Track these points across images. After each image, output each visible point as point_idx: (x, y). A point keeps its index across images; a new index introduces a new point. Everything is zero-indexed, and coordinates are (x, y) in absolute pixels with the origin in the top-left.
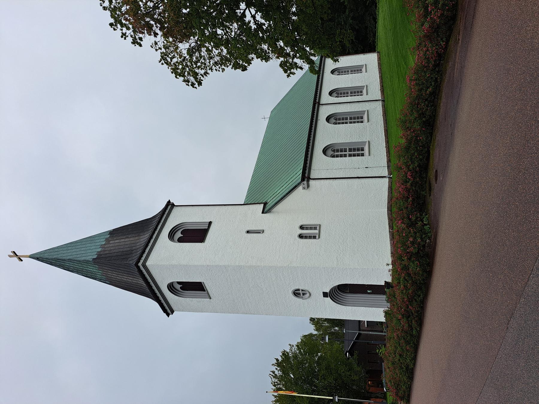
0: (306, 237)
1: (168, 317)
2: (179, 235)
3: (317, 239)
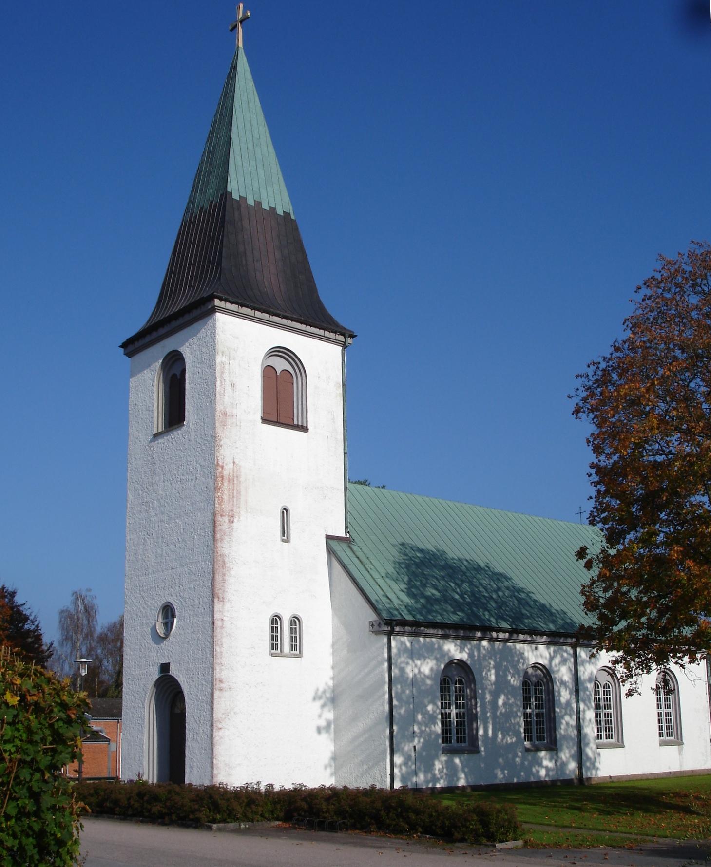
0: (273, 630)
1: (120, 347)
2: (280, 365)
3: (270, 651)
